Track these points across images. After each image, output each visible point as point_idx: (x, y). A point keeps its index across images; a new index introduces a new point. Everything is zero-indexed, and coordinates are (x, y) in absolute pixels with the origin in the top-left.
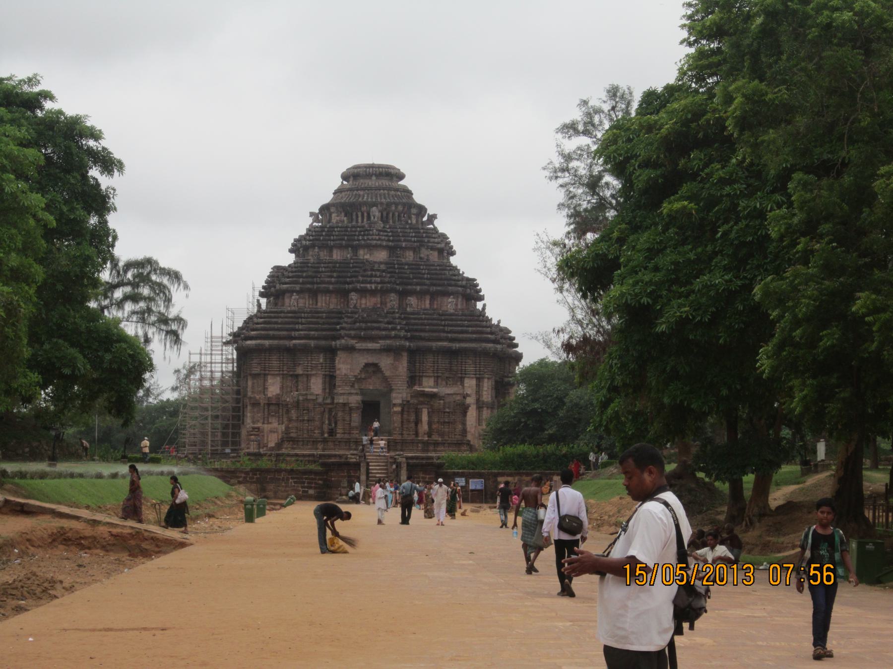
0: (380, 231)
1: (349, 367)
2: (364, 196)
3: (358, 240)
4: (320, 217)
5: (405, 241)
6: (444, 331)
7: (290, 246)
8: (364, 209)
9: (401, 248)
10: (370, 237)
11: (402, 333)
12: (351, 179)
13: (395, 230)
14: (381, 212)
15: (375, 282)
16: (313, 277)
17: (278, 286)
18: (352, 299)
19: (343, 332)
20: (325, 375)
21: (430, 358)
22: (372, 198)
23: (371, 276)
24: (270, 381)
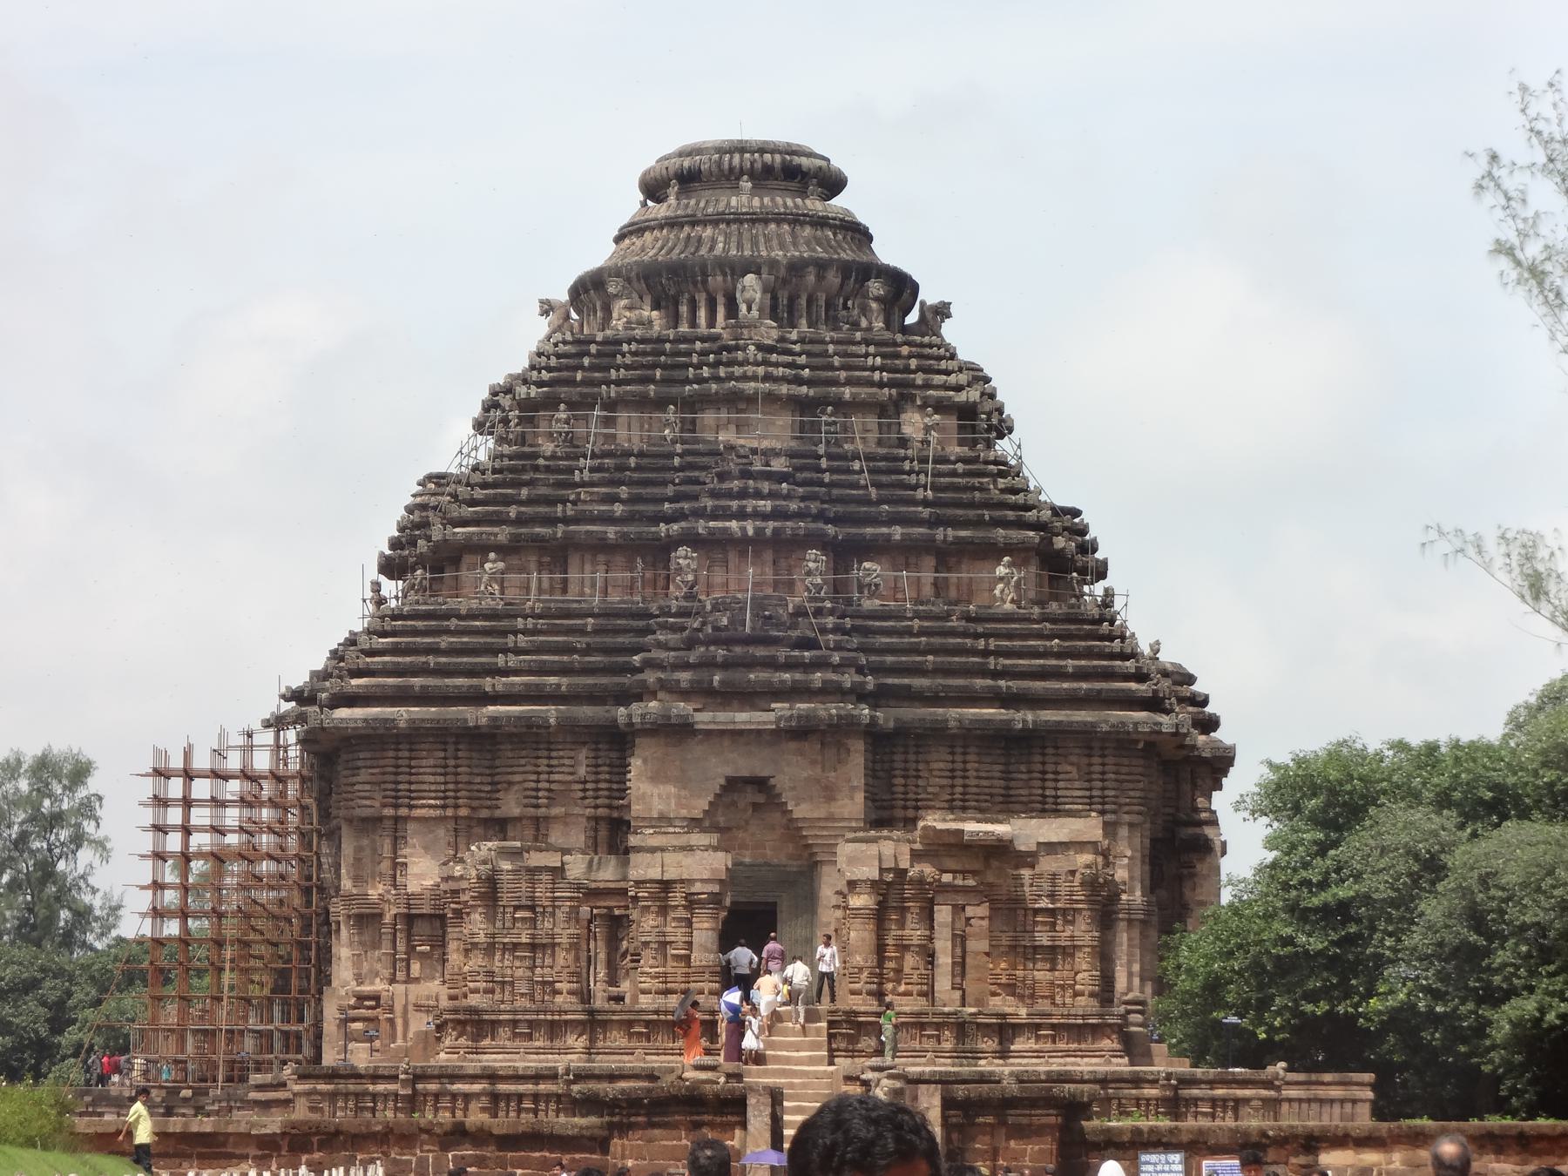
0: (770, 349)
2: (714, 241)
3: (700, 380)
4: (574, 315)
5: (849, 382)
6: (984, 672)
7: (476, 411)
8: (716, 281)
9: (840, 406)
10: (738, 371)
11: (848, 679)
12: (673, 191)
13: (817, 348)
14: (771, 291)
15: (757, 515)
16: (551, 502)
17: (437, 533)
18: (680, 570)
19: (651, 677)
20: (589, 818)
21: (939, 760)
22: (740, 246)
23: (743, 494)
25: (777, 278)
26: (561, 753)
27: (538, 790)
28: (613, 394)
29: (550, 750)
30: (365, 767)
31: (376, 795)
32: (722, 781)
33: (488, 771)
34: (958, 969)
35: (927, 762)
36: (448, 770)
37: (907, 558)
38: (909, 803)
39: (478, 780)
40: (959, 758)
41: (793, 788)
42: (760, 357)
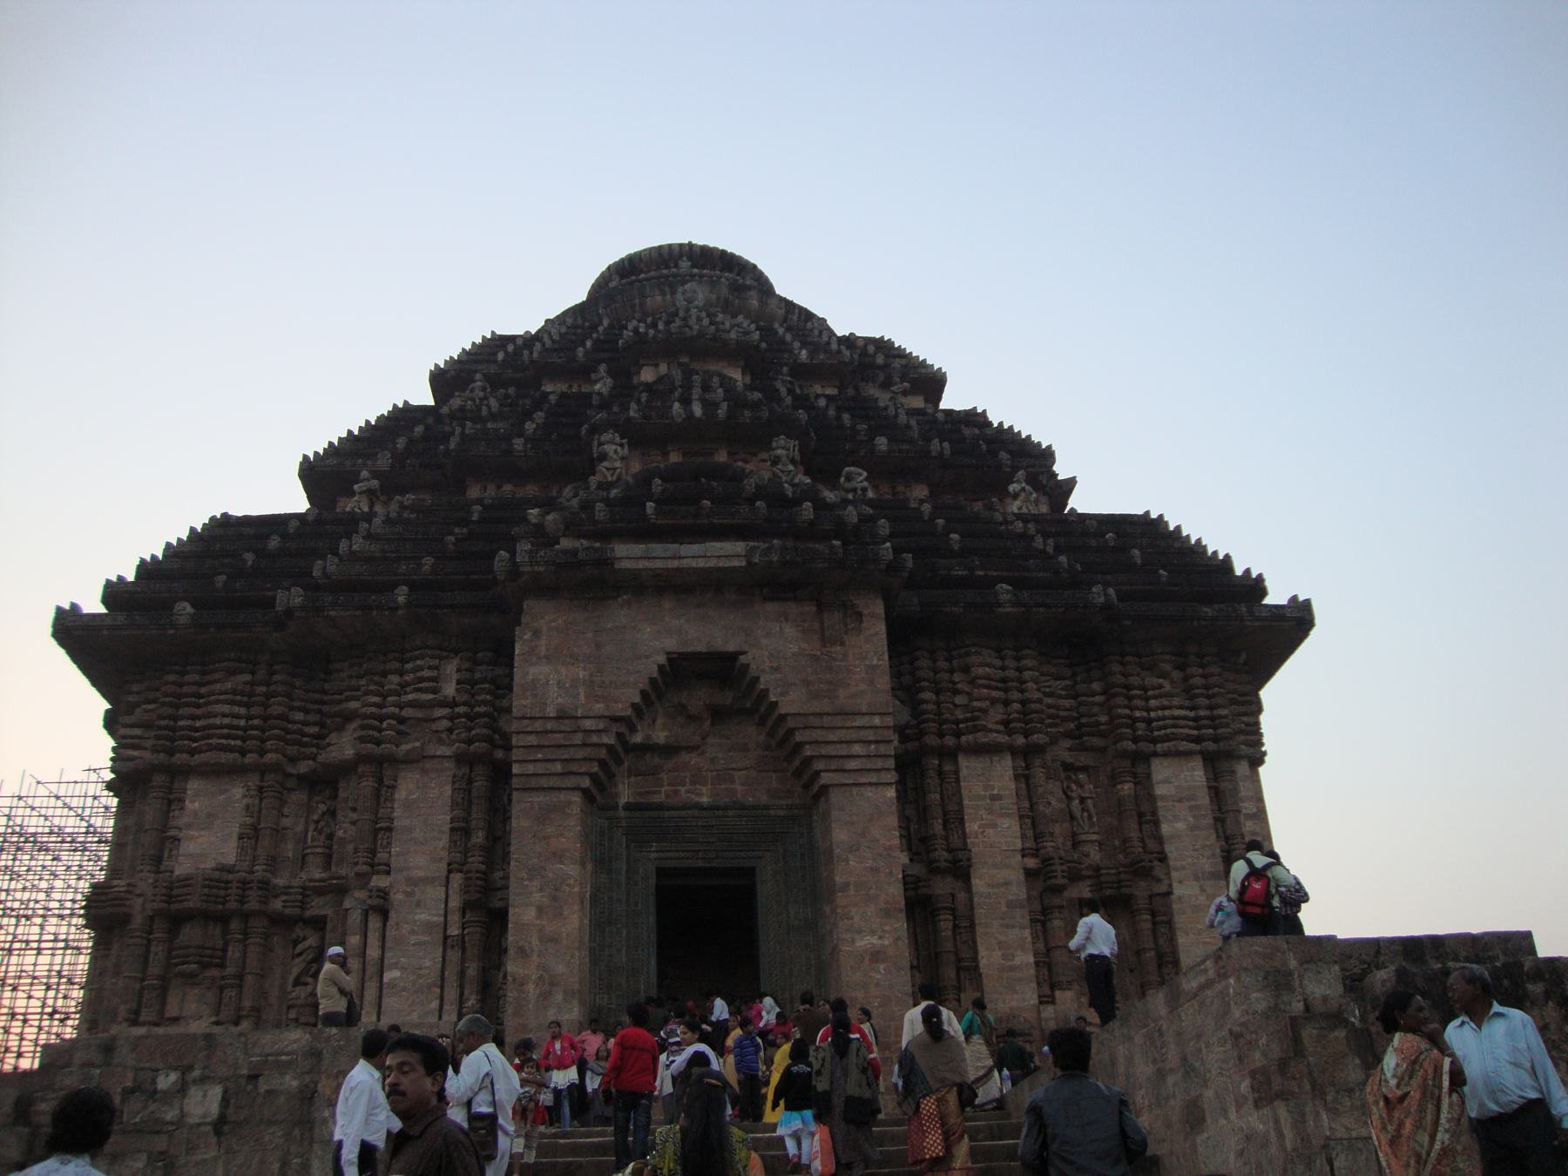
1: (582, 674)
18: (603, 457)
20: (459, 759)
24: (193, 805)
25: (718, 299)
26: (418, 662)
27: (381, 719)
28: (535, 355)
29: (404, 661)
30: (138, 705)
31: (149, 743)
32: (662, 659)
33: (316, 707)
34: (1045, 971)
35: (966, 670)
36: (253, 699)
37: (894, 488)
38: (945, 727)
39: (299, 716)
40: (1010, 663)
41: (777, 669)
42: (704, 314)
